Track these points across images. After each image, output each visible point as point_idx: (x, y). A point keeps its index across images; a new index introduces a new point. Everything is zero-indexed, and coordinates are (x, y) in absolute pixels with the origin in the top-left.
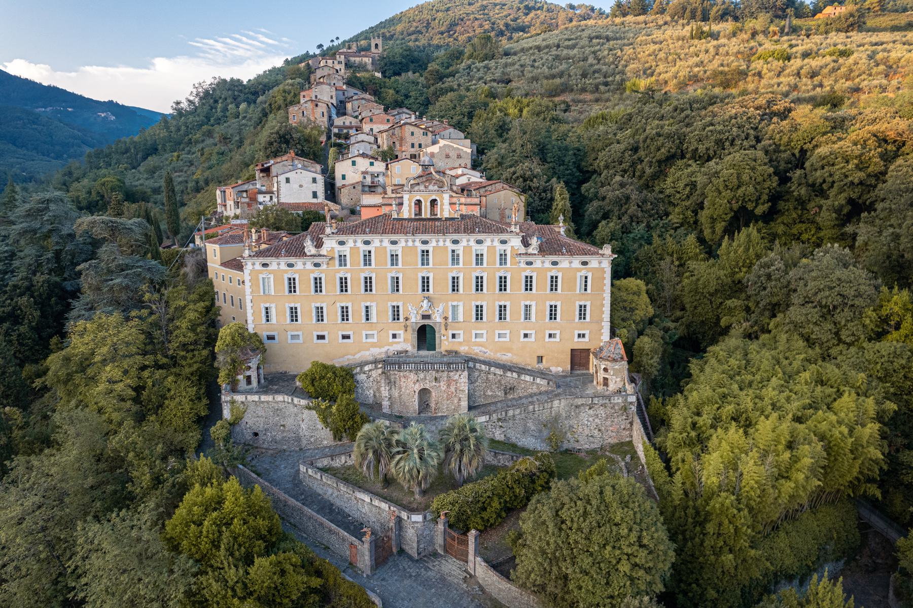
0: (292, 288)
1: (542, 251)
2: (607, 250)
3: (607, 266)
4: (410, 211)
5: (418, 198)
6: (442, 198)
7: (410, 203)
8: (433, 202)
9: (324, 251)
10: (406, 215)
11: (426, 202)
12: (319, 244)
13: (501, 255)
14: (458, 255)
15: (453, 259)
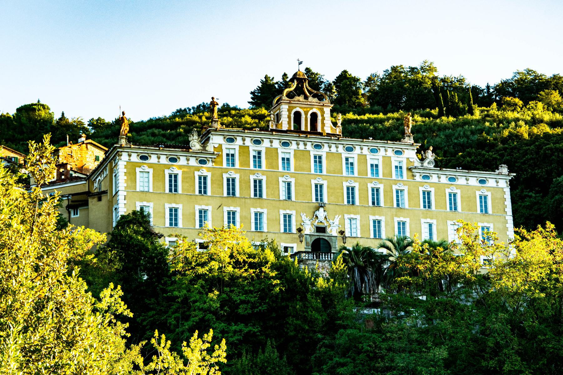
0: (173, 187)
1: (439, 165)
2: (504, 170)
3: (504, 184)
4: (289, 123)
5: (298, 109)
6: (323, 113)
7: (290, 113)
8: (314, 116)
9: (210, 148)
10: (285, 127)
11: (306, 113)
12: (204, 140)
13: (396, 167)
14: (352, 164)
15: (347, 168)
